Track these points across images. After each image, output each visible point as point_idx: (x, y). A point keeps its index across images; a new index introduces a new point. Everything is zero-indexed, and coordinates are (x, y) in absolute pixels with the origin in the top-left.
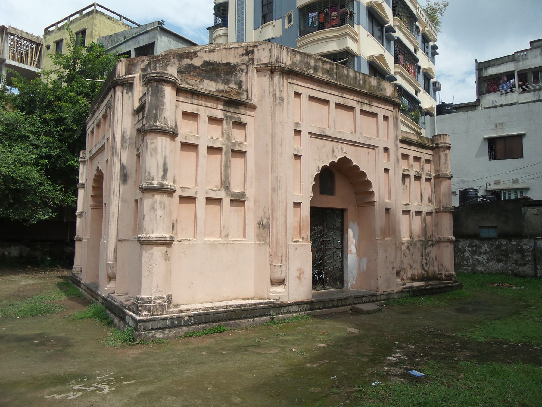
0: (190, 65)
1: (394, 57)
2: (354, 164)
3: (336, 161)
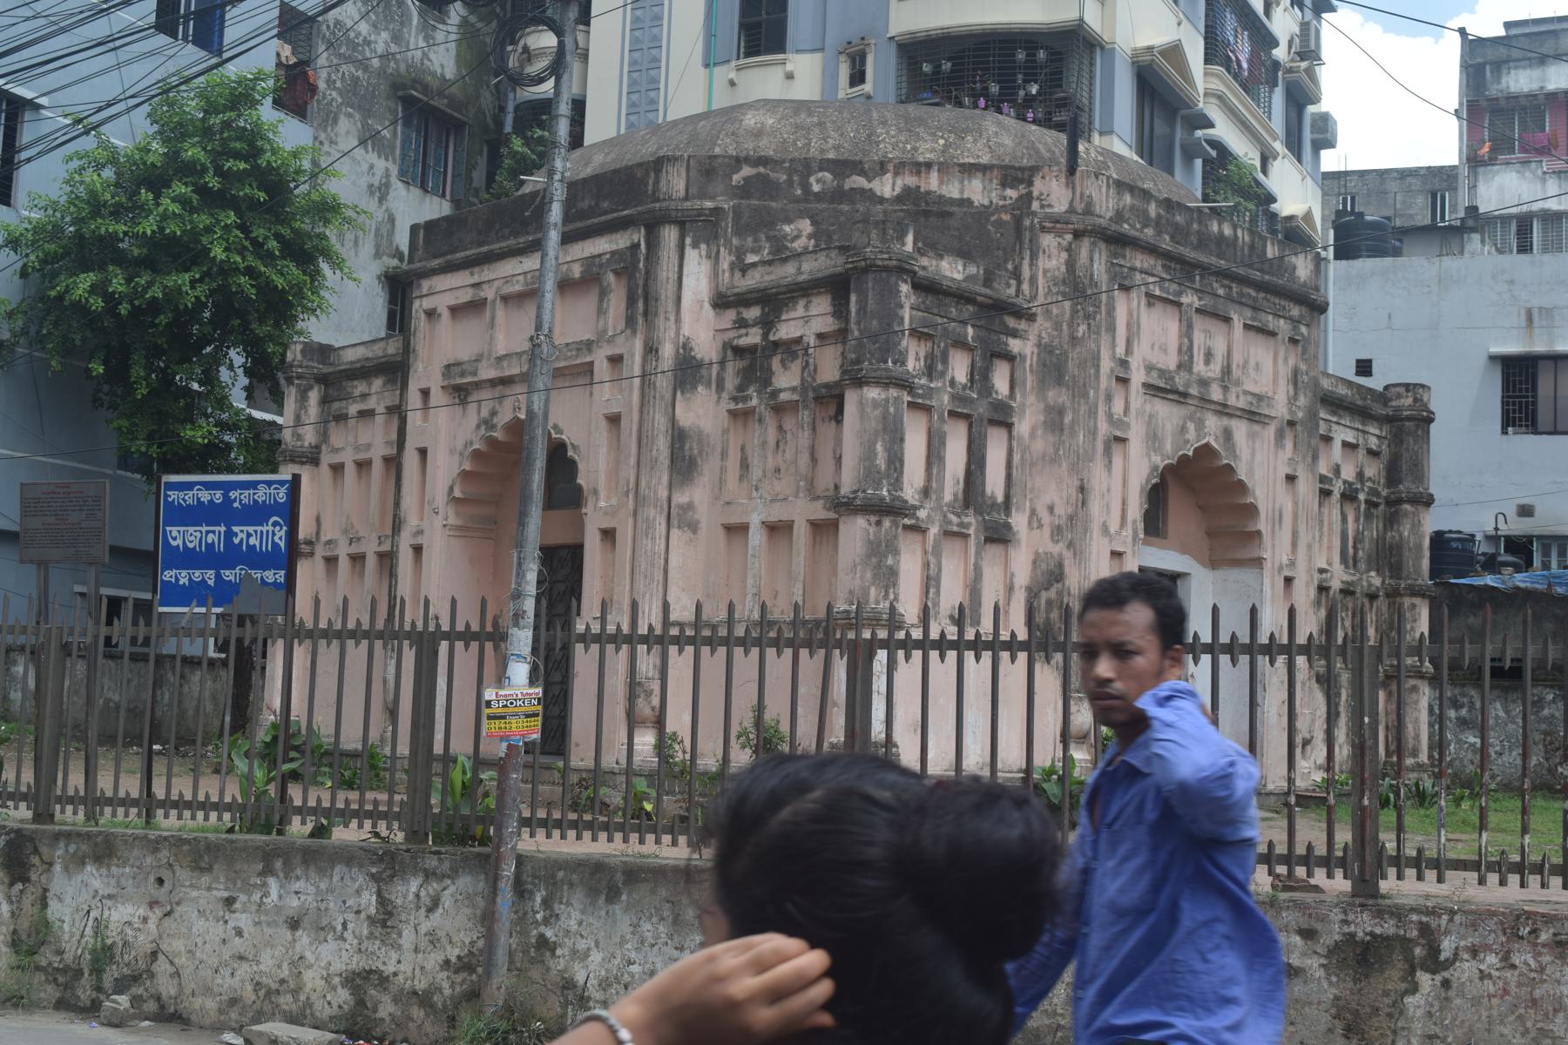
0: (869, 196)
1: (1206, 38)
2: (1226, 461)
3: (1191, 453)
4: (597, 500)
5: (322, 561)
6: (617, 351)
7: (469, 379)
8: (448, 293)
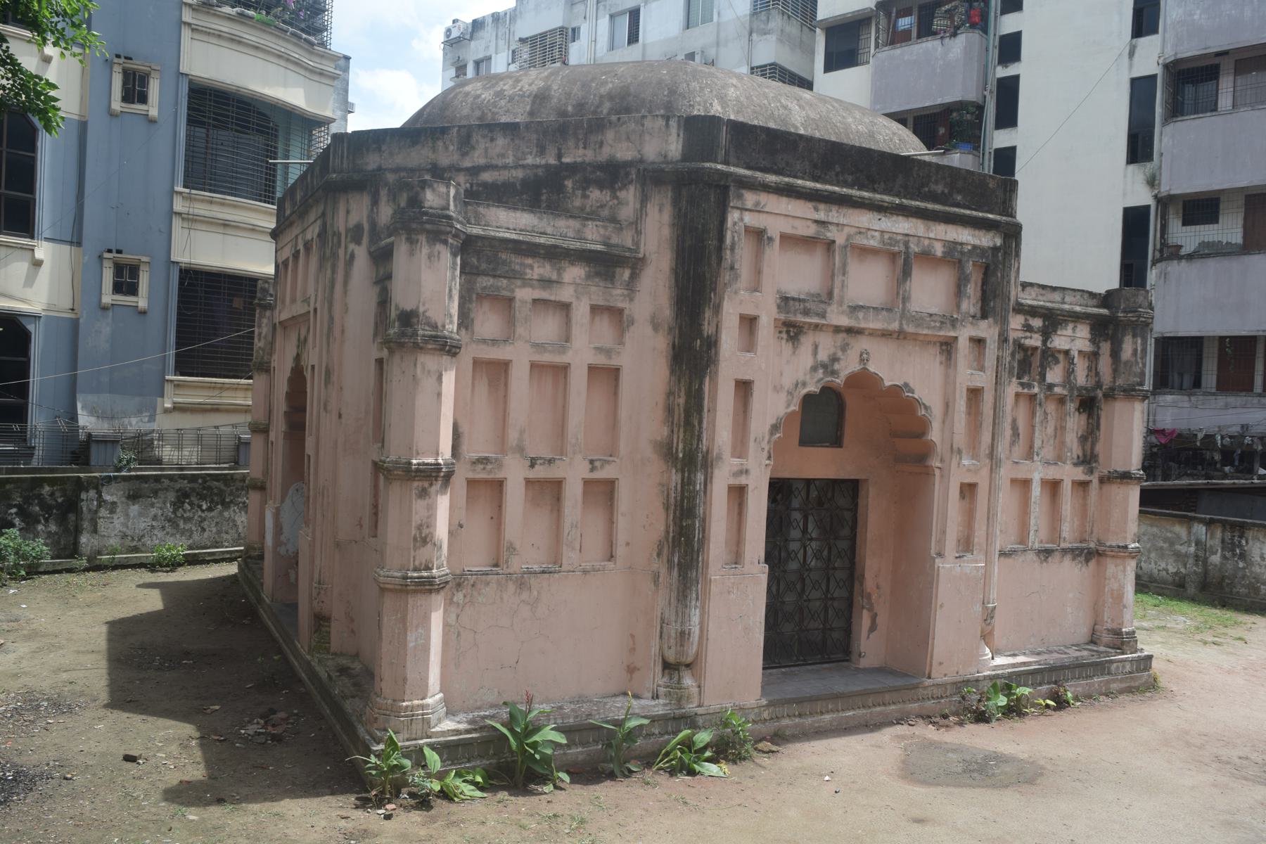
4: (961, 458)
5: (465, 484)
6: (981, 334)
7: (815, 320)
8: (782, 218)
